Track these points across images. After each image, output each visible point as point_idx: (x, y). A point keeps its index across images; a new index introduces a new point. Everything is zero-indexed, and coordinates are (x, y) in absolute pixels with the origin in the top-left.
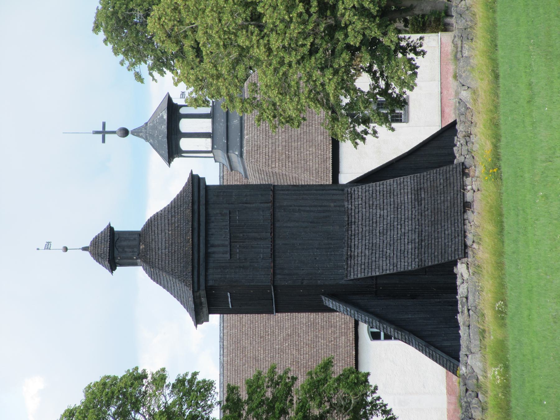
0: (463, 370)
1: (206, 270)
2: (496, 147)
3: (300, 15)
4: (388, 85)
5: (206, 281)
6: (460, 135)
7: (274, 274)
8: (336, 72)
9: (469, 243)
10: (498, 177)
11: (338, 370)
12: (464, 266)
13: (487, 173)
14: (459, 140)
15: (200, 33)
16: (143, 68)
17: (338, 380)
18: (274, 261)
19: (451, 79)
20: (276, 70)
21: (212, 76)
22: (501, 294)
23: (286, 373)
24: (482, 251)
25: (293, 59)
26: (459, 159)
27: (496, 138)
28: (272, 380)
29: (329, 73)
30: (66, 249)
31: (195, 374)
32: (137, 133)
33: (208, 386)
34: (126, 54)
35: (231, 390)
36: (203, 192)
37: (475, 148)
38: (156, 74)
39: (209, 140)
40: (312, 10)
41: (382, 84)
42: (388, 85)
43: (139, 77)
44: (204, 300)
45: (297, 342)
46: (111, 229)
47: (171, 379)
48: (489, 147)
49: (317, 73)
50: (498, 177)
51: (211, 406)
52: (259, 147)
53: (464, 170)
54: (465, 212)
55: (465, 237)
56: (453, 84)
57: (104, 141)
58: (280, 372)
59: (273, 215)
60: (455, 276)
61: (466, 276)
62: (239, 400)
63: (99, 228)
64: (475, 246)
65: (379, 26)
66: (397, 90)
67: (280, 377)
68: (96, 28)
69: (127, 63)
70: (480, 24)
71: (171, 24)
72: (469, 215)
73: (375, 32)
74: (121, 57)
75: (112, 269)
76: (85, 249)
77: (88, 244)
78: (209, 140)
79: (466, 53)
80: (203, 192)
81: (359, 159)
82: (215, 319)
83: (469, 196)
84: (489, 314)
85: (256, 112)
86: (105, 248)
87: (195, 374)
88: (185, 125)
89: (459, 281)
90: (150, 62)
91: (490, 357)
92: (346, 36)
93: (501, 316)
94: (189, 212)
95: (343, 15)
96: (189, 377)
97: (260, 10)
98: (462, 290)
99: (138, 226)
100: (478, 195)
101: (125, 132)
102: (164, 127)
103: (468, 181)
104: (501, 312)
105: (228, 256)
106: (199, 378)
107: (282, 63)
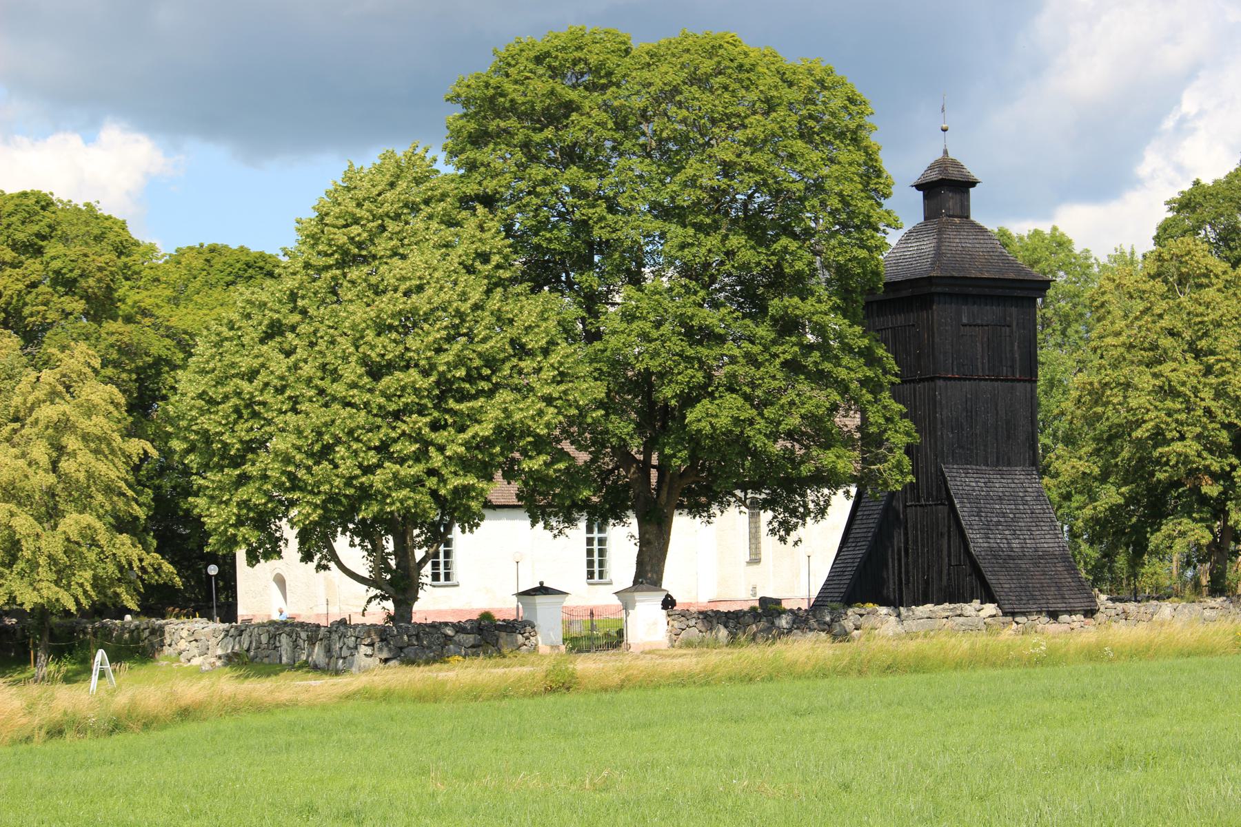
5: (939, 294)
7: (945, 379)
9: (1017, 619)
12: (994, 612)
18: (959, 379)
20: (1184, 384)
24: (1010, 634)
29: (1196, 446)
30: (945, 130)
49: (1199, 430)
55: (1024, 614)
59: (1006, 380)
61: (982, 614)
72: (1044, 619)
76: (946, 152)
77: (951, 156)
83: (1064, 618)
86: (954, 174)
94: (1012, 276)
105: (965, 321)
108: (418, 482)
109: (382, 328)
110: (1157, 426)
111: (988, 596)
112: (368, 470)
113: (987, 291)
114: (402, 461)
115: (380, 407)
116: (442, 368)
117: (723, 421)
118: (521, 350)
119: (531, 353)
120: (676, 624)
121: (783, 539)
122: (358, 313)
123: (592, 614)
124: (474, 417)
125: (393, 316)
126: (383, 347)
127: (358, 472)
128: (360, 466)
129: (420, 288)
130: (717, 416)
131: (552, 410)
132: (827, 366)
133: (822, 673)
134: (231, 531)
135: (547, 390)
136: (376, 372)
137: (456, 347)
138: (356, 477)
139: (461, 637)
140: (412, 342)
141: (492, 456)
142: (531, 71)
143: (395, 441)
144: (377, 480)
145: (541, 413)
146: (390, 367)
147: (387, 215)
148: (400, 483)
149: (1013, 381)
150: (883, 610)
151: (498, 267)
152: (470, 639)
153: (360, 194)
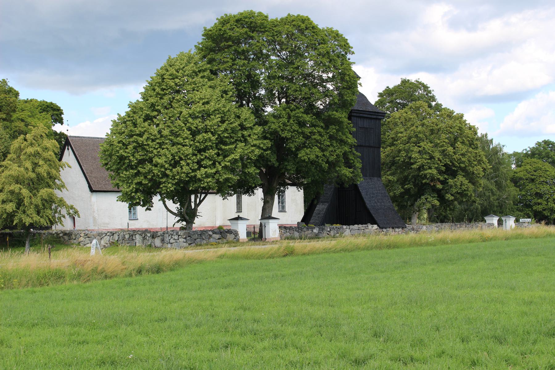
36: (380, 117)
55: (386, 228)
80: (380, 117)
83: (397, 230)
103: (400, 229)
108: (212, 176)
109: (195, 118)
110: (422, 164)
111: (374, 222)
112: (194, 171)
113: (361, 115)
117: (312, 157)
123: (254, 228)
124: (231, 152)
125: (200, 112)
126: (197, 123)
127: (191, 171)
130: (310, 155)
133: (368, 248)
134: (133, 194)
135: (255, 142)
137: (225, 124)
138: (190, 173)
139: (214, 236)
140: (207, 122)
142: (236, 25)
143: (203, 160)
144: (199, 174)
148: (207, 176)
149: (374, 147)
150: (345, 227)
152: (217, 236)
153: (177, 67)
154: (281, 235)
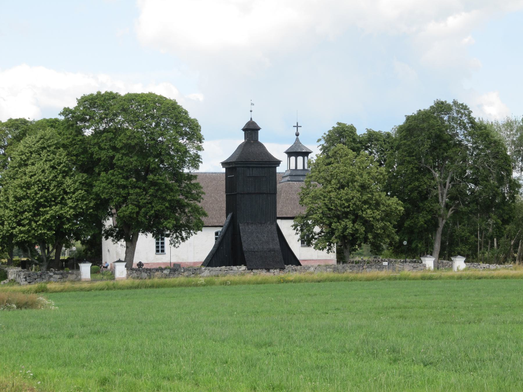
0: (203, 268)
1: (243, 167)
2: (291, 281)
3: (344, 204)
4: (316, 239)
5: (239, 167)
6: (296, 267)
7: (241, 194)
8: (321, 218)
9: (254, 271)
10: (279, 282)
11: (203, 219)
13: (281, 278)
14: (294, 267)
15: (337, 165)
16: (323, 142)
17: (199, 219)
19: (318, 264)
20: (322, 195)
21: (319, 169)
22: (233, 283)
23: (202, 198)
24: (250, 276)
25: (326, 201)
26: (287, 267)
27: (295, 282)
28: (199, 193)
29: (321, 215)
30: (251, 111)
31: (202, 162)
32: (297, 140)
33: (197, 167)
34: (328, 135)
35: (195, 177)
36: (274, 166)
37: (291, 273)
38: (321, 147)
39: (294, 168)
40: (346, 209)
41: (316, 237)
42: (316, 239)
43: (319, 140)
44: (231, 166)
45: (214, 203)
46: (259, 129)
47: (199, 153)
48: (291, 278)
50: (279, 282)
51: (189, 168)
52: (291, 188)
53: (282, 269)
54: (266, 269)
56: (316, 264)
57: (294, 126)
58: (203, 196)
60: (240, 265)
61: (240, 269)
62: (191, 180)
63: (259, 124)
64: (252, 273)
65: (339, 235)
66: (314, 242)
67: (200, 196)
68: (339, 124)
69: (325, 136)
70: (340, 275)
71: (340, 153)
73: (337, 234)
74: (327, 133)
75: (244, 130)
76: (251, 119)
77: (253, 120)
78: (294, 168)
79: (328, 270)
80: (274, 166)
81: (287, 228)
82: (224, 170)
83: (272, 271)
84: (225, 278)
85: (305, 187)
86: (252, 127)
87: (202, 162)
88: (300, 159)
89: (238, 267)
90: (325, 145)
91: (209, 279)
92: (336, 222)
93: (225, 283)
94: (266, 160)
95: (344, 221)
96: (200, 160)
97: (346, 188)
98: (235, 268)
99: (260, 140)
100: (272, 274)
101: (297, 135)
102: (299, 150)
103: (278, 270)
104: (226, 283)
106: (200, 164)
107: (325, 197)
108: (29, 231)
111: (245, 265)
112: (14, 228)
114: (24, 226)
115: (19, 210)
116: (37, 199)
118: (66, 193)
119: (69, 193)
120: (129, 272)
121: (174, 246)
122: (17, 182)
124: (46, 212)
126: (20, 193)
127: (9, 229)
128: (11, 227)
129: (35, 175)
130: (126, 211)
131: (72, 210)
132: (164, 195)
135: (71, 205)
136: (18, 199)
138: (10, 230)
139: (55, 276)
141: (51, 224)
143: (23, 220)
145: (68, 211)
146: (23, 198)
147: (34, 151)
148: (21, 232)
151: (64, 166)
154: (128, 275)
